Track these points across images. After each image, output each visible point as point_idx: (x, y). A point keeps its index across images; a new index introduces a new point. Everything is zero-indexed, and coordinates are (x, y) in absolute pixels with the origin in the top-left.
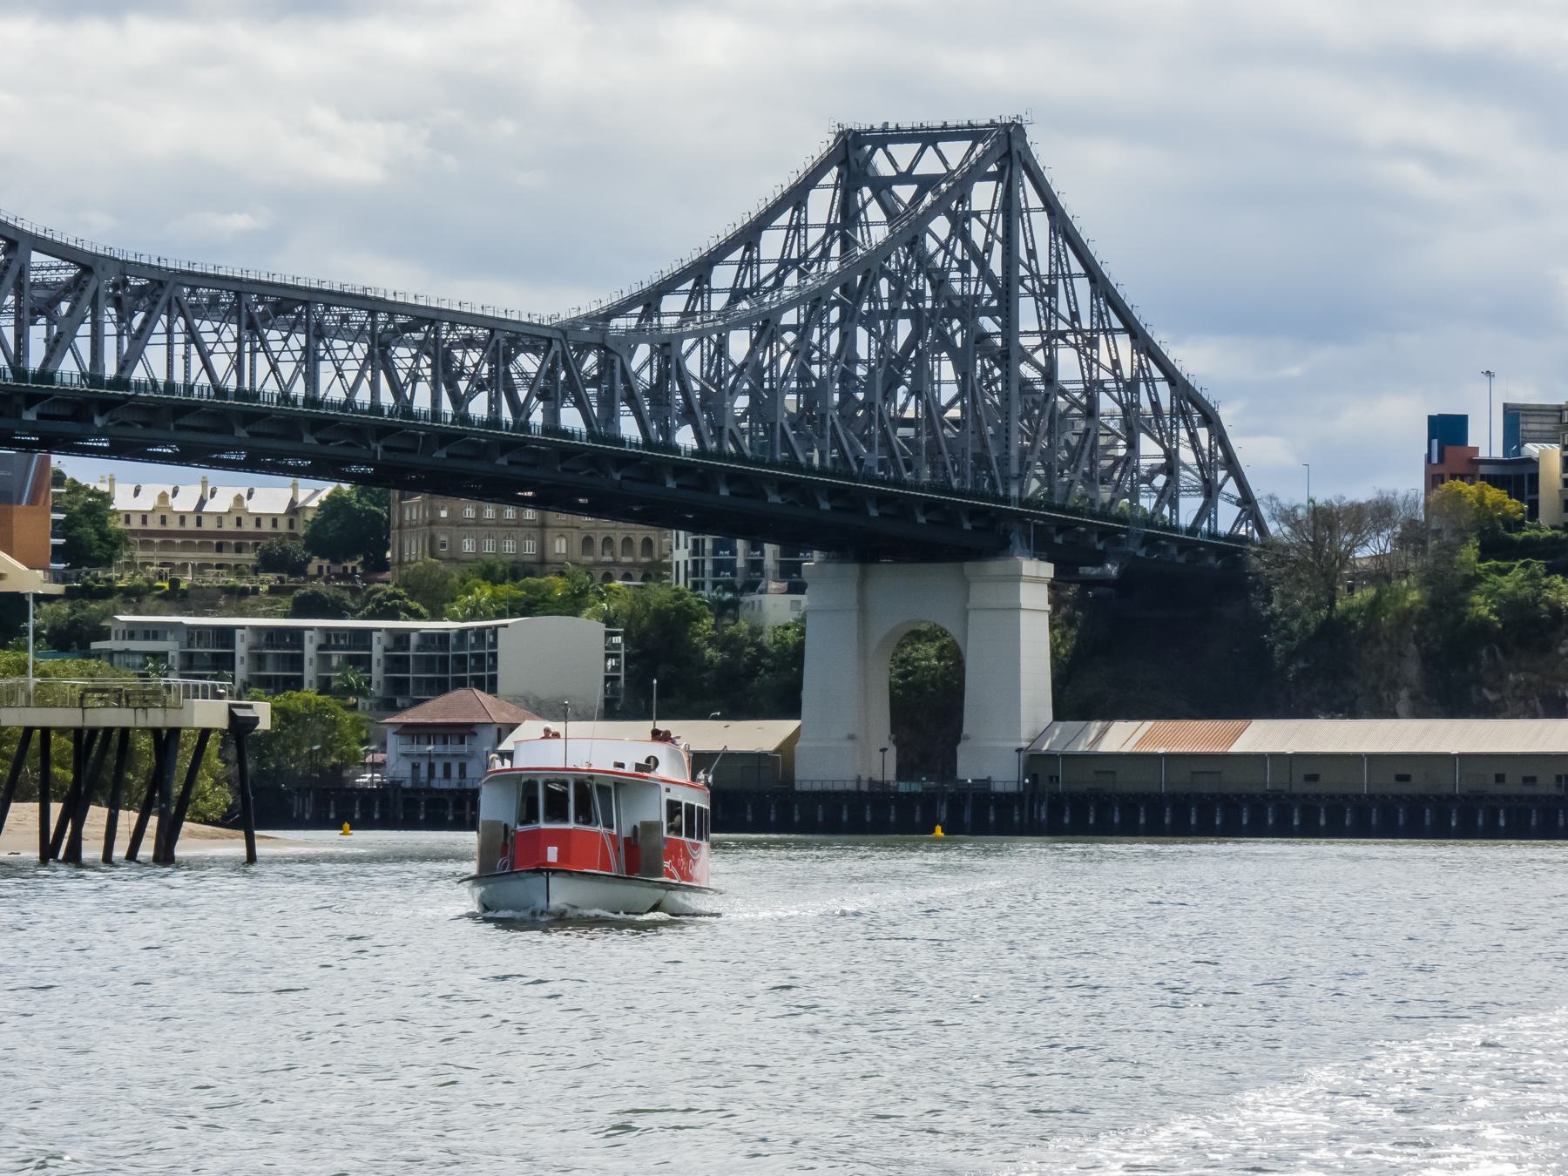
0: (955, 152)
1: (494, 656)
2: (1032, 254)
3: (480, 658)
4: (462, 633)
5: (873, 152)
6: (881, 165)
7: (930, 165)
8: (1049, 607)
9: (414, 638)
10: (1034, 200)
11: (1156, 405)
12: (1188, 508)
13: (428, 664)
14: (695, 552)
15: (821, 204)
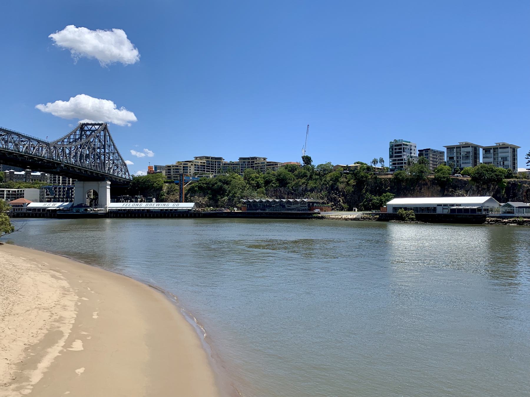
0: (97, 127)
1: (23, 194)
2: (107, 141)
3: (21, 194)
4: (18, 191)
5: (85, 127)
6: (86, 128)
7: (93, 128)
8: (110, 188)
9: (11, 191)
10: (108, 135)
11: (120, 163)
12: (124, 176)
13: (12, 194)
14: (50, 181)
15: (78, 132)
